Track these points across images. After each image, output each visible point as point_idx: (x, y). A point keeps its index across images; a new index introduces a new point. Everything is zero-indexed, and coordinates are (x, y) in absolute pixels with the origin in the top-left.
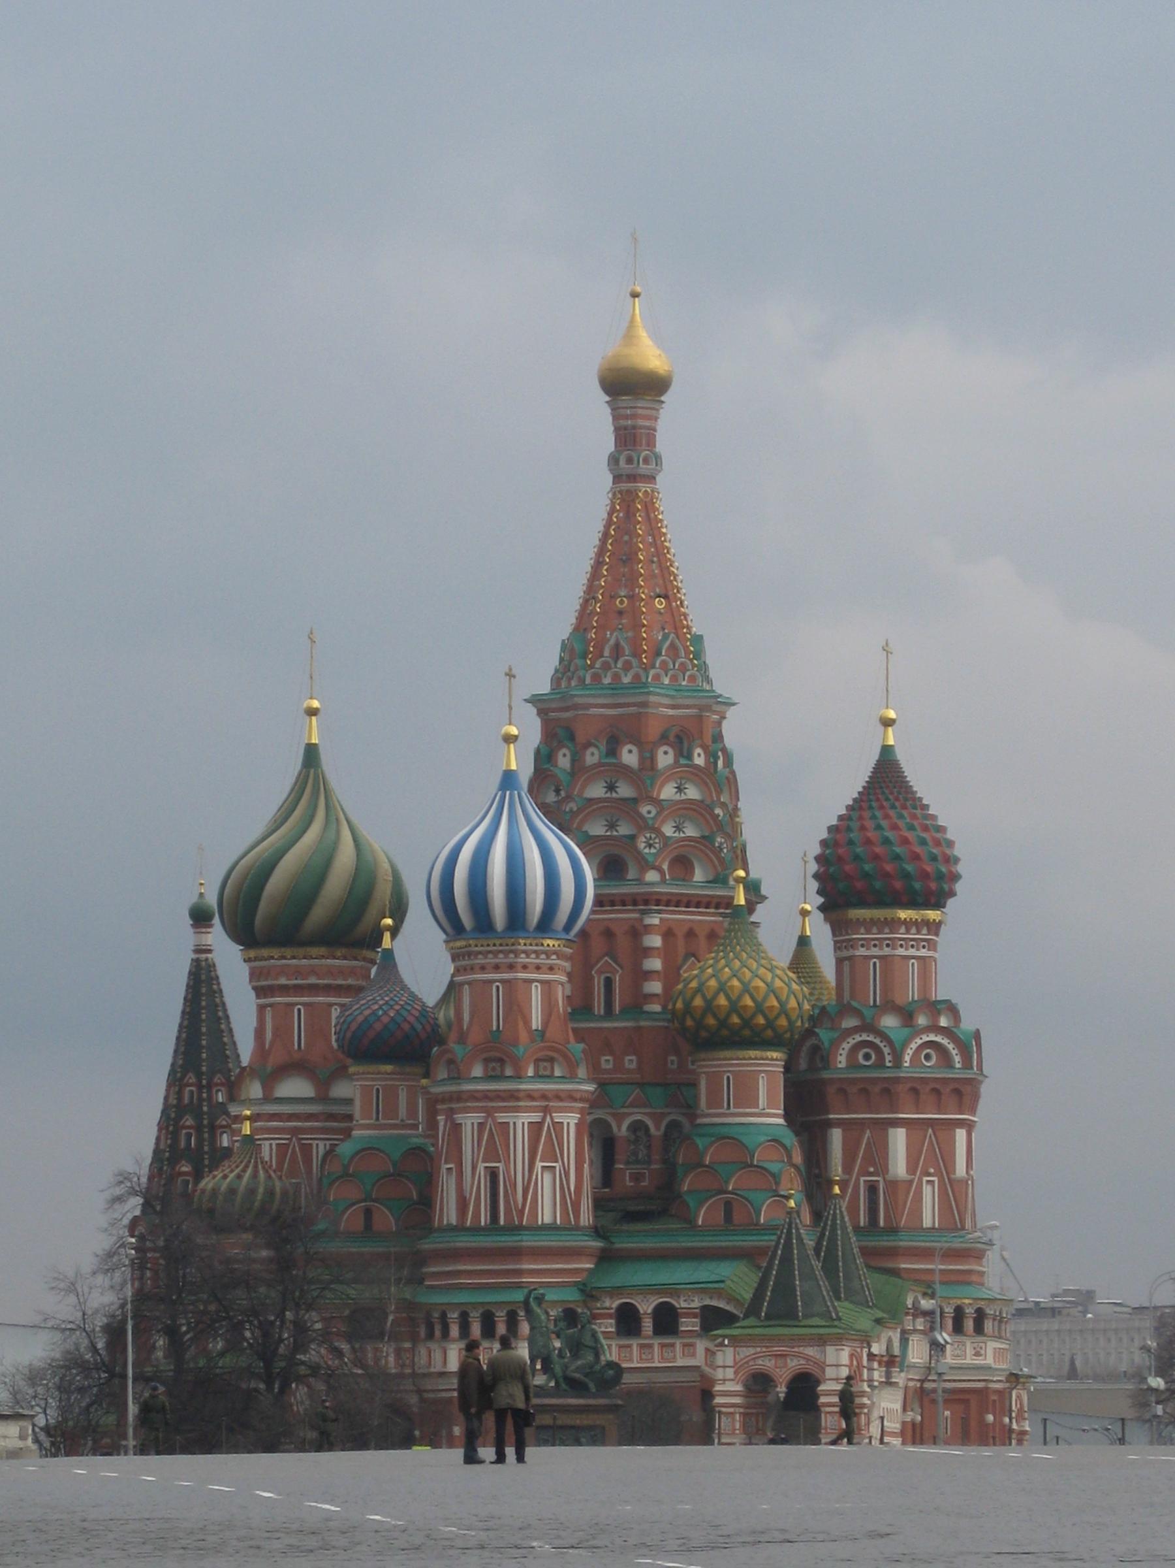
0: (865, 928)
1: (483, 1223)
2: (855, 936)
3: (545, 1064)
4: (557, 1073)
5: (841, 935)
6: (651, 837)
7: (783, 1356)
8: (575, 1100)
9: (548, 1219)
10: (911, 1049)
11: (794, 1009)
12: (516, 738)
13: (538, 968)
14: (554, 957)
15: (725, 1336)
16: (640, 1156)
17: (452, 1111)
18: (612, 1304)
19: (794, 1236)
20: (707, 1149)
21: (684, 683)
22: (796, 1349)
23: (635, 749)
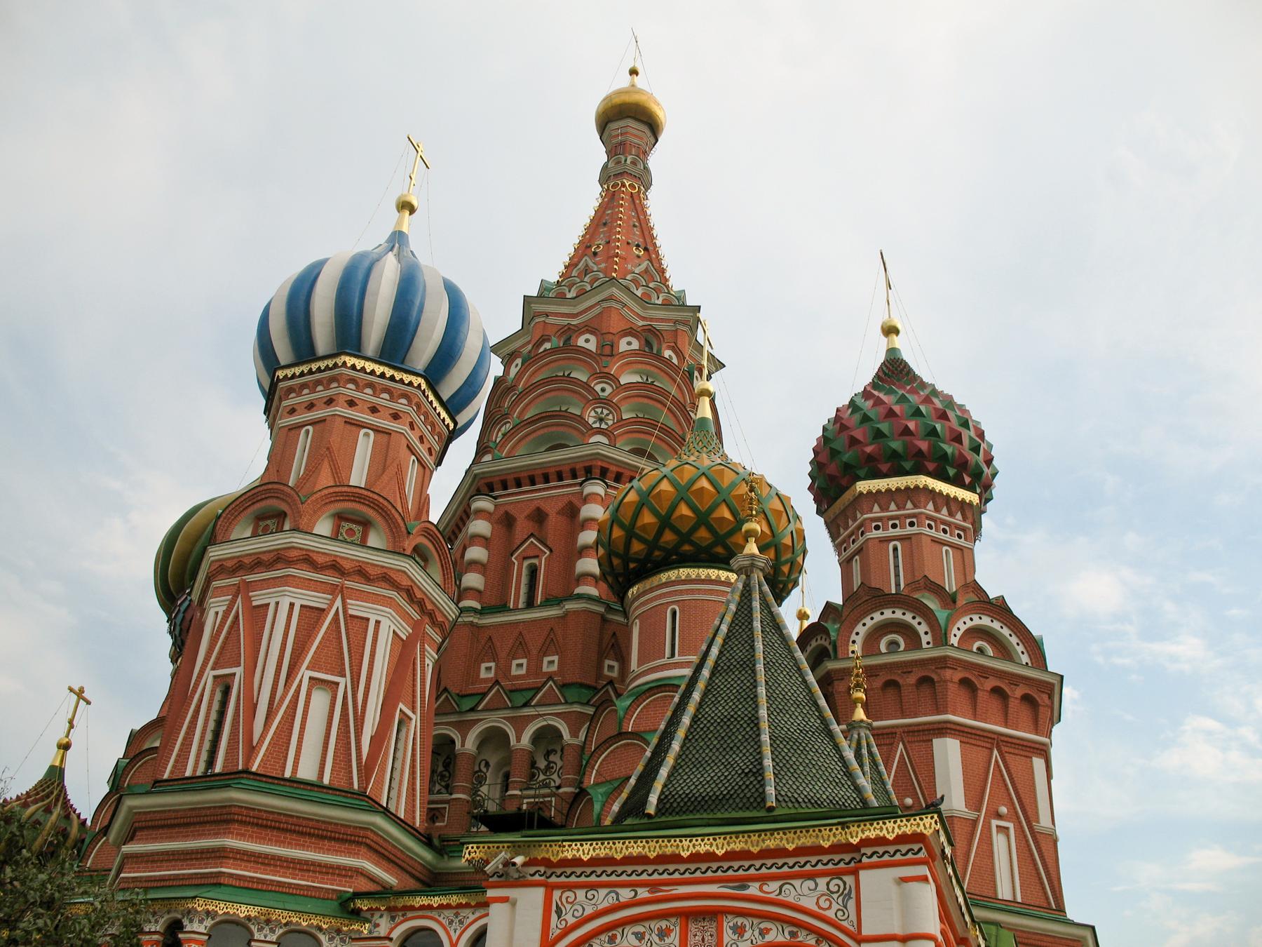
0: (879, 505)
1: (188, 773)
2: (865, 516)
3: (353, 526)
4: (373, 540)
5: (846, 528)
6: (602, 413)
7: (714, 915)
8: (395, 586)
9: (307, 771)
10: (959, 629)
11: (778, 513)
12: (412, 210)
13: (374, 410)
14: (404, 401)
15: (517, 848)
16: (553, 784)
17: (203, 611)
18: (392, 930)
19: (757, 615)
20: (629, 710)
21: (660, 302)
22: (753, 889)
23: (593, 339)
